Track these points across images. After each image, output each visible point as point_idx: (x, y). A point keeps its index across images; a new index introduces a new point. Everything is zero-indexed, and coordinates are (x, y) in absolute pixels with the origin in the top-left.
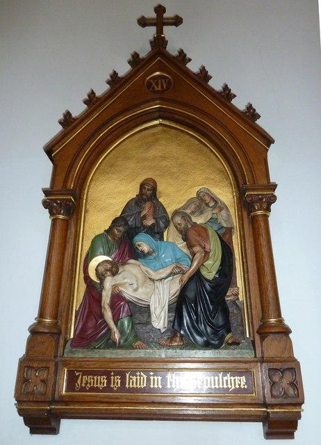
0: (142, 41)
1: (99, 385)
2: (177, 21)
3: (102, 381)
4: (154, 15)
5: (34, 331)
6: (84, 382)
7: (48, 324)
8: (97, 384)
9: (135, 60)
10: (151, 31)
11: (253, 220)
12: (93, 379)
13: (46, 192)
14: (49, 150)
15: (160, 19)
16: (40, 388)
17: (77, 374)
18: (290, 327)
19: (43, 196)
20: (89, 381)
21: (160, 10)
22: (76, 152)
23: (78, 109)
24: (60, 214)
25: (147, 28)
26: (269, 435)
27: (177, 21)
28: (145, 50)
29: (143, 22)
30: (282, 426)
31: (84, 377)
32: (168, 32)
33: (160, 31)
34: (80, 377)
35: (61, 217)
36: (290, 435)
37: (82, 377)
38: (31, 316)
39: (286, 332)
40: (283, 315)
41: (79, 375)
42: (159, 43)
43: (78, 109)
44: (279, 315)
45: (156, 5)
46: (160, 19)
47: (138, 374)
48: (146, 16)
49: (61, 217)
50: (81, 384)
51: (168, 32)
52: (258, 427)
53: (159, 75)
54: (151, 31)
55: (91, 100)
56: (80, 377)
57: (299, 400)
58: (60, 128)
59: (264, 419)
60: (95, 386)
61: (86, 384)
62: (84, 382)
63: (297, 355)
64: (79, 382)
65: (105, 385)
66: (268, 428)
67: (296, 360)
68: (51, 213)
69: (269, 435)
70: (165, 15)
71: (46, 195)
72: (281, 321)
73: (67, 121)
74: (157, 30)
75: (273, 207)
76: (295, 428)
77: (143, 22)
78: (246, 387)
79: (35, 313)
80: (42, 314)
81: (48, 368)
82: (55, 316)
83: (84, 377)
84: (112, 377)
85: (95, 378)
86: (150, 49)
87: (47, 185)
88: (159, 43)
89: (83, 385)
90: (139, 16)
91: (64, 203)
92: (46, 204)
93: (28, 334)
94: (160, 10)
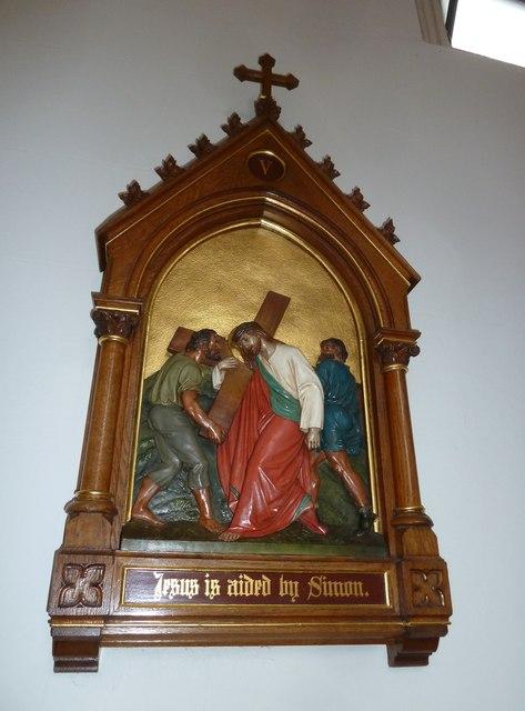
1: (187, 593)
2: (290, 82)
4: (258, 68)
5: (74, 511)
9: (233, 125)
10: (253, 90)
13: (94, 295)
14: (102, 235)
15: (265, 74)
16: (90, 596)
17: (157, 576)
18: (432, 518)
19: (89, 306)
21: (267, 61)
23: (149, 181)
26: (398, 660)
27: (290, 82)
28: (247, 115)
29: (242, 74)
30: (413, 647)
32: (278, 93)
34: (160, 581)
35: (115, 338)
36: (422, 660)
39: (428, 523)
43: (149, 181)
44: (417, 499)
45: (262, 53)
46: (265, 74)
47: (241, 577)
48: (249, 67)
51: (278, 93)
52: (380, 652)
53: (269, 156)
54: (253, 90)
55: (168, 169)
56: (160, 581)
58: (121, 204)
60: (182, 594)
61: (169, 591)
62: (166, 588)
63: (443, 554)
69: (398, 660)
70: (275, 70)
71: (96, 303)
72: (420, 511)
73: (133, 195)
76: (434, 648)
77: (242, 74)
82: (106, 485)
84: (207, 581)
86: (254, 115)
87: (98, 290)
88: (267, 109)
90: (238, 65)
94: (267, 61)
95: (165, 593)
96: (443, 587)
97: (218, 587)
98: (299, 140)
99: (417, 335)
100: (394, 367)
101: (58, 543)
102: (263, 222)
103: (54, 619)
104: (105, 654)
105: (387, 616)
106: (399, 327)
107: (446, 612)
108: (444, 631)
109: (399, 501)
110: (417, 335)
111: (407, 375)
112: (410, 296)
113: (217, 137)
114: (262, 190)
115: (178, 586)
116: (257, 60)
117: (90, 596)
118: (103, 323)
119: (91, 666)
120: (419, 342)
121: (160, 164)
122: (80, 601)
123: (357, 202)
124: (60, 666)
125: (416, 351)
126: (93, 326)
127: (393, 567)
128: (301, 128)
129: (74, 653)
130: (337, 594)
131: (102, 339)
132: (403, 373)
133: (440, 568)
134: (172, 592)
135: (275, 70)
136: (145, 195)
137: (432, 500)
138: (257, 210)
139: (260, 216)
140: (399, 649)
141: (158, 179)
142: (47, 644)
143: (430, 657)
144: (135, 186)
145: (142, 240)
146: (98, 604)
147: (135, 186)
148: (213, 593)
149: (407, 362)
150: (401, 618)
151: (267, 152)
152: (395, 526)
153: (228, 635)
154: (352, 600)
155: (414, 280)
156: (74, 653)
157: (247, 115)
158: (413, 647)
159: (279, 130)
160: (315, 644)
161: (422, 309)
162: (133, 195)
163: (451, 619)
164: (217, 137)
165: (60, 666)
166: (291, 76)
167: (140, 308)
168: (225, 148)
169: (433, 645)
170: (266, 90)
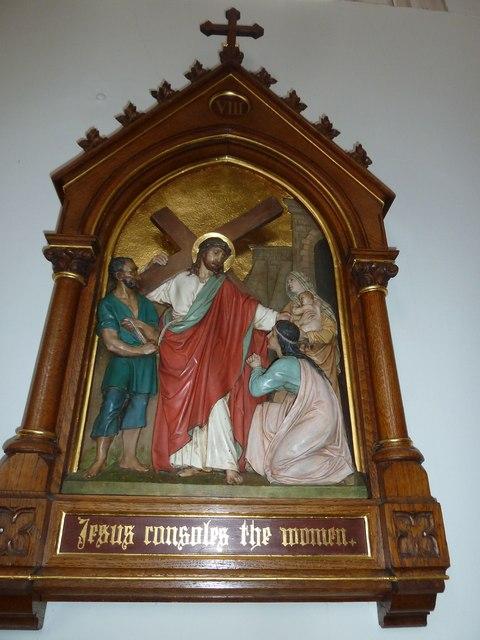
0: (209, 53)
1: (119, 541)
2: (256, 32)
4: (224, 21)
6: (92, 534)
7: (38, 438)
9: (196, 73)
10: (220, 41)
11: (363, 300)
12: (109, 530)
13: (48, 235)
14: (59, 180)
15: (232, 28)
17: (82, 521)
19: (44, 243)
20: (101, 534)
21: (233, 15)
22: (103, 191)
26: (389, 621)
27: (256, 32)
28: (211, 62)
29: (208, 29)
31: (92, 527)
32: (243, 43)
33: (231, 41)
34: (86, 527)
35: (71, 275)
36: (420, 620)
39: (418, 458)
41: (83, 525)
42: (231, 56)
46: (232, 28)
48: (215, 21)
49: (71, 275)
51: (243, 43)
52: (370, 611)
54: (220, 41)
56: (86, 527)
58: (80, 150)
59: (379, 595)
60: (113, 542)
61: (96, 538)
64: (83, 534)
65: (131, 542)
66: (392, 607)
67: (433, 501)
68: (57, 269)
69: (389, 621)
70: (239, 23)
71: (49, 242)
72: (406, 441)
74: (228, 40)
75: (391, 282)
76: (432, 607)
77: (208, 29)
83: (92, 527)
87: (52, 227)
88: (231, 56)
89: (91, 540)
90: (203, 21)
91: (83, 260)
92: (49, 254)
94: (233, 15)
95: (91, 540)
96: (437, 532)
97: (132, 534)
98: (264, 80)
99: (394, 253)
108: (442, 589)
109: (380, 433)
110: (394, 253)
111: (387, 299)
112: (388, 221)
113: (179, 83)
118: (56, 256)
119: (33, 623)
120: (398, 262)
123: (326, 130)
125: (394, 271)
127: (376, 510)
130: (320, 543)
132: (382, 295)
133: (431, 509)
134: (100, 540)
135: (239, 23)
137: (418, 438)
141: (118, 126)
144: (94, 133)
147: (94, 133)
148: (181, 541)
149: (384, 284)
150: (388, 571)
151: (230, 93)
152: (377, 462)
153: (114, 590)
154: (335, 549)
155: (389, 198)
157: (211, 62)
161: (397, 228)
163: (448, 572)
166: (256, 26)
167: (94, 244)
169: (430, 604)
170: (231, 41)
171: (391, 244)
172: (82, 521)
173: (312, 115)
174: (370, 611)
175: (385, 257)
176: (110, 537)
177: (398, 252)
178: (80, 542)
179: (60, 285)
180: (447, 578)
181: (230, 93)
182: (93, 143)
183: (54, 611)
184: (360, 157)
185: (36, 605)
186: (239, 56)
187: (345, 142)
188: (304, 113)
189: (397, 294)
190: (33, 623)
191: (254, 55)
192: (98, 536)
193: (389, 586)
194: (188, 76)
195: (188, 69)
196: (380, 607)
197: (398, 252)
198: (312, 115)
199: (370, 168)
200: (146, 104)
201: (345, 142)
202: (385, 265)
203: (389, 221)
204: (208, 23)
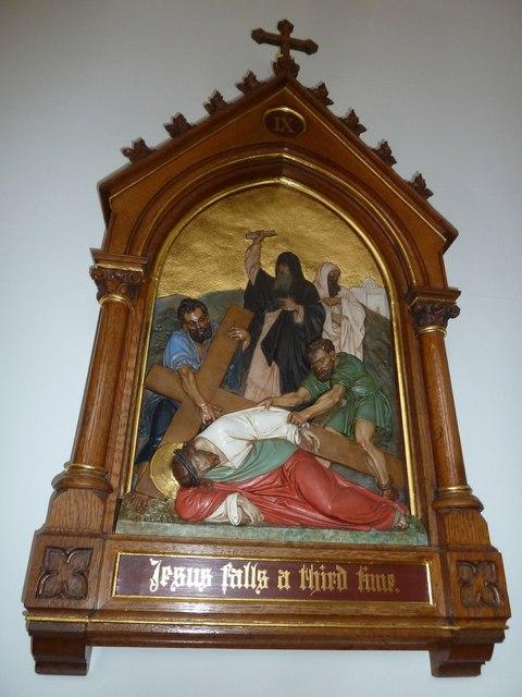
0: (263, 62)
2: (309, 47)
3: (203, 578)
4: (278, 33)
5: (62, 485)
6: (165, 578)
8: (193, 580)
9: (248, 84)
10: (272, 53)
11: (421, 337)
12: (185, 572)
13: (96, 255)
14: (106, 190)
16: (74, 584)
17: (153, 563)
19: (90, 262)
21: (285, 27)
24: (116, 291)
25: (265, 46)
26: (442, 670)
27: (309, 47)
28: (265, 74)
29: (260, 37)
30: (463, 653)
32: (297, 56)
34: (157, 571)
35: (118, 298)
36: (472, 669)
37: (161, 570)
38: (57, 452)
39: (477, 507)
40: (470, 481)
42: (286, 69)
46: (282, 37)
49: (118, 298)
50: (160, 580)
51: (297, 56)
52: (422, 660)
54: (272, 53)
55: (178, 126)
57: (502, 614)
58: (125, 161)
60: (189, 584)
61: (170, 582)
62: (165, 578)
63: (494, 543)
66: (450, 658)
70: (292, 35)
71: (96, 261)
73: (138, 152)
76: (489, 658)
77: (260, 37)
78: (397, 590)
79: (67, 456)
80: (78, 454)
81: (91, 549)
83: (164, 569)
85: (190, 570)
87: (98, 245)
88: (286, 69)
89: (164, 583)
90: (256, 27)
92: (98, 276)
93: (51, 490)
94: (285, 27)
95: (164, 583)
96: (498, 582)
98: (320, 97)
99: (457, 293)
100: (430, 329)
101: (39, 519)
102: (284, 180)
103: (31, 610)
104: (97, 655)
105: (431, 616)
106: (439, 285)
107: (502, 614)
108: (501, 638)
109: (440, 480)
110: (457, 293)
112: (446, 257)
113: (231, 95)
114: (279, 146)
115: (183, 576)
116: (276, 24)
117: (74, 584)
119: (78, 667)
120: (459, 302)
121: (169, 121)
122: (62, 592)
123: (384, 156)
124: (43, 667)
125: (455, 312)
126: (94, 289)
128: (324, 84)
129: (58, 651)
131: (102, 300)
132: (440, 339)
133: (491, 561)
134: (175, 582)
136: (149, 151)
137: (480, 482)
138: (276, 169)
139: (280, 175)
140: (445, 656)
141: (165, 137)
142: (27, 640)
143: (483, 667)
145: (150, 200)
146: (84, 595)
147: (140, 144)
149: (444, 325)
150: (450, 620)
151: (286, 109)
155: (451, 235)
156: (58, 651)
157: (265, 74)
158: (463, 653)
159: (297, 88)
160: (365, 649)
161: (458, 267)
162: (138, 152)
163: (508, 623)
164: (231, 95)
165: (43, 667)
167: (144, 266)
168: (240, 106)
169: (487, 654)
170: (285, 52)
171: (451, 283)
172: (153, 563)
173: (370, 139)
174: (422, 660)
175: (447, 297)
176: (186, 579)
177: (460, 292)
178: (152, 584)
179: (107, 309)
180: (507, 628)
181: (286, 109)
182: (138, 152)
183: (97, 655)
184: (419, 190)
185: (87, 648)
186: (295, 69)
187: (405, 170)
188: (363, 137)
189: (458, 337)
190: (78, 667)
191: (309, 73)
192: (172, 577)
193: (448, 635)
194: (239, 86)
195: (240, 80)
196: (432, 658)
197: (460, 292)
198: (370, 139)
199: (430, 200)
200: (196, 115)
201: (405, 170)
202: (444, 304)
203: (449, 258)
204: (260, 31)
